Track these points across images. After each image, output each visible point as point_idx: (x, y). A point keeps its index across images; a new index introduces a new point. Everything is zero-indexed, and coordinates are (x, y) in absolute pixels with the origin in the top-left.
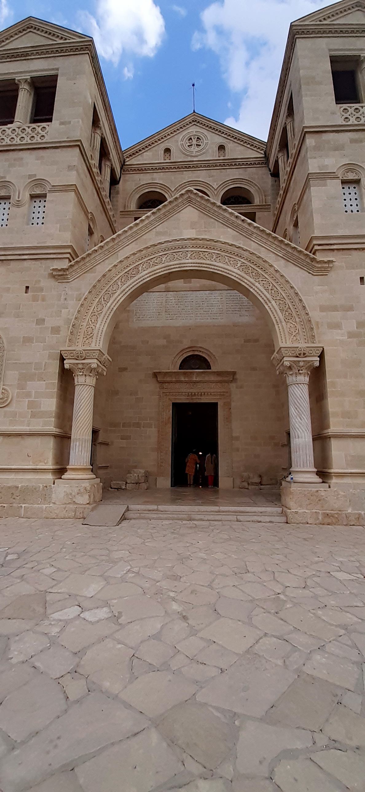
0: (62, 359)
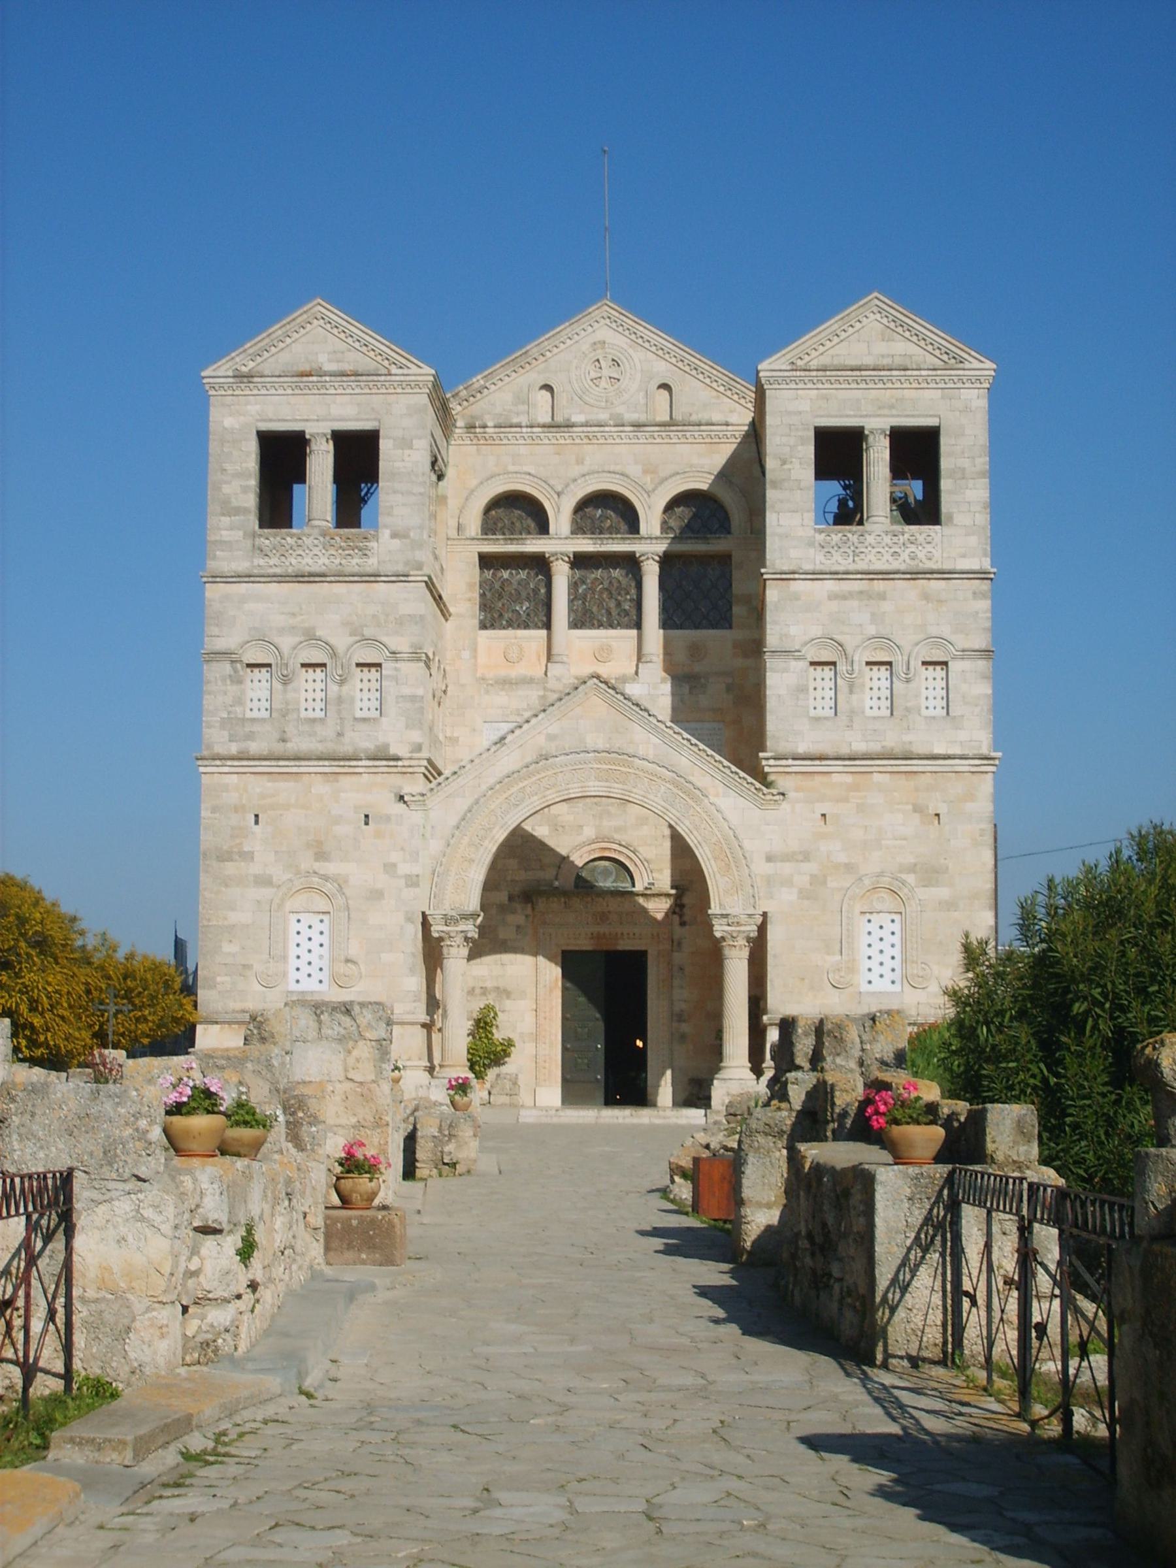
0: (426, 924)
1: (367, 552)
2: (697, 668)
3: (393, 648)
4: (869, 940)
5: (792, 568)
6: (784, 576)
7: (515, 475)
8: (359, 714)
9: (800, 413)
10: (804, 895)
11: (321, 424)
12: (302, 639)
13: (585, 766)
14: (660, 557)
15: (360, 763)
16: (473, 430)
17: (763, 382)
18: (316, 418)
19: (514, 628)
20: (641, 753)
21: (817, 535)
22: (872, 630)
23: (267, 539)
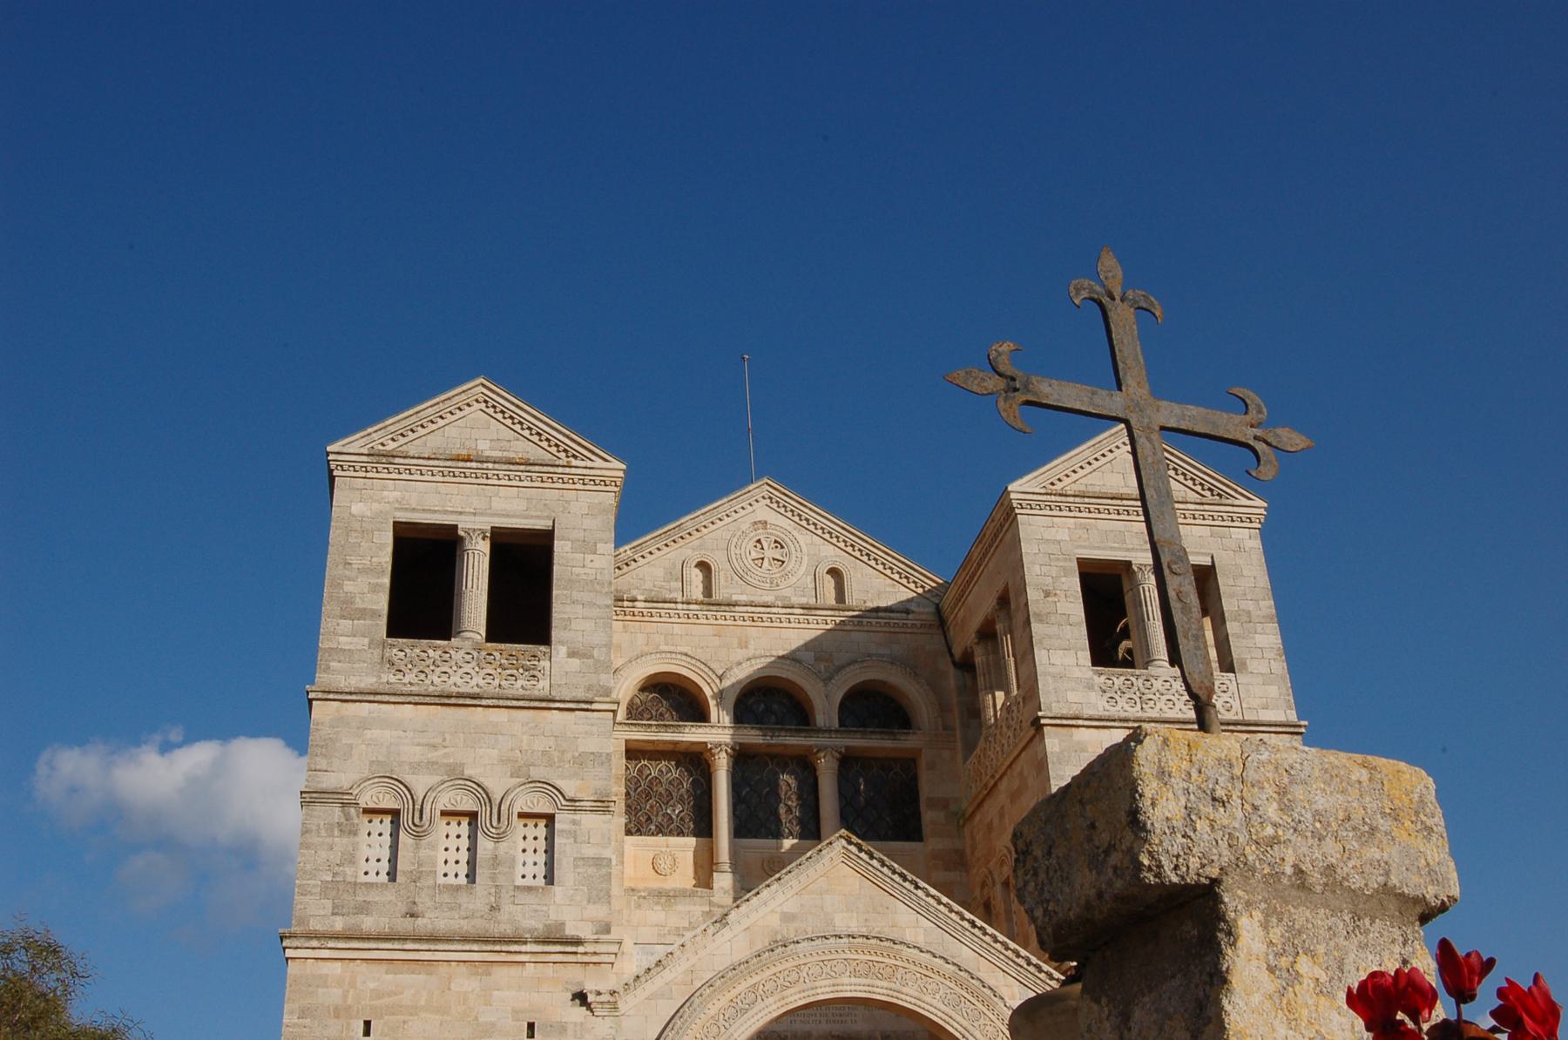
1: (536, 673)
3: (570, 794)
5: (1071, 713)
6: (1065, 722)
7: (669, 655)
8: (519, 882)
11: (478, 519)
12: (446, 778)
13: (837, 956)
14: (840, 753)
15: (523, 948)
16: (620, 603)
17: (1015, 505)
18: (472, 511)
19: (664, 834)
20: (909, 938)
21: (1096, 677)
23: (402, 651)
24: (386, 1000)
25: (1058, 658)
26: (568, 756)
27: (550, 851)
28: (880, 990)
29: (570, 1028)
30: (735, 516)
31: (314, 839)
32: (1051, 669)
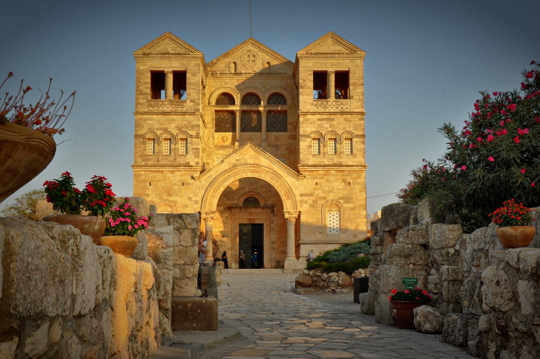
2: (278, 143)
3: (191, 134)
4: (330, 219)
8: (180, 153)
9: (309, 67)
10: (311, 206)
11: (169, 69)
20: (263, 165)
22: (330, 129)
24: (154, 179)
25: (305, 97)
26: (190, 125)
27: (186, 146)
28: (256, 176)
29: (191, 184)
30: (243, 49)
31: (137, 146)
32: (304, 101)
